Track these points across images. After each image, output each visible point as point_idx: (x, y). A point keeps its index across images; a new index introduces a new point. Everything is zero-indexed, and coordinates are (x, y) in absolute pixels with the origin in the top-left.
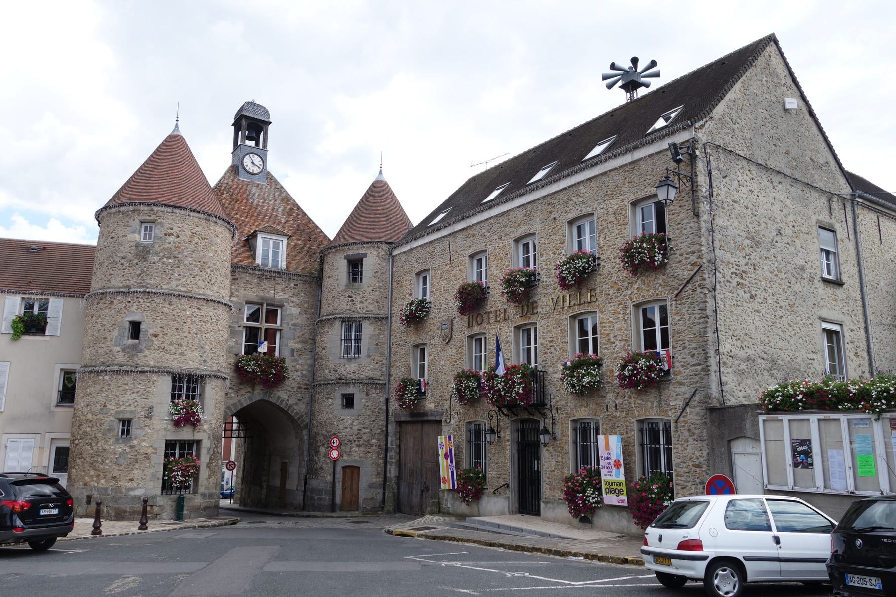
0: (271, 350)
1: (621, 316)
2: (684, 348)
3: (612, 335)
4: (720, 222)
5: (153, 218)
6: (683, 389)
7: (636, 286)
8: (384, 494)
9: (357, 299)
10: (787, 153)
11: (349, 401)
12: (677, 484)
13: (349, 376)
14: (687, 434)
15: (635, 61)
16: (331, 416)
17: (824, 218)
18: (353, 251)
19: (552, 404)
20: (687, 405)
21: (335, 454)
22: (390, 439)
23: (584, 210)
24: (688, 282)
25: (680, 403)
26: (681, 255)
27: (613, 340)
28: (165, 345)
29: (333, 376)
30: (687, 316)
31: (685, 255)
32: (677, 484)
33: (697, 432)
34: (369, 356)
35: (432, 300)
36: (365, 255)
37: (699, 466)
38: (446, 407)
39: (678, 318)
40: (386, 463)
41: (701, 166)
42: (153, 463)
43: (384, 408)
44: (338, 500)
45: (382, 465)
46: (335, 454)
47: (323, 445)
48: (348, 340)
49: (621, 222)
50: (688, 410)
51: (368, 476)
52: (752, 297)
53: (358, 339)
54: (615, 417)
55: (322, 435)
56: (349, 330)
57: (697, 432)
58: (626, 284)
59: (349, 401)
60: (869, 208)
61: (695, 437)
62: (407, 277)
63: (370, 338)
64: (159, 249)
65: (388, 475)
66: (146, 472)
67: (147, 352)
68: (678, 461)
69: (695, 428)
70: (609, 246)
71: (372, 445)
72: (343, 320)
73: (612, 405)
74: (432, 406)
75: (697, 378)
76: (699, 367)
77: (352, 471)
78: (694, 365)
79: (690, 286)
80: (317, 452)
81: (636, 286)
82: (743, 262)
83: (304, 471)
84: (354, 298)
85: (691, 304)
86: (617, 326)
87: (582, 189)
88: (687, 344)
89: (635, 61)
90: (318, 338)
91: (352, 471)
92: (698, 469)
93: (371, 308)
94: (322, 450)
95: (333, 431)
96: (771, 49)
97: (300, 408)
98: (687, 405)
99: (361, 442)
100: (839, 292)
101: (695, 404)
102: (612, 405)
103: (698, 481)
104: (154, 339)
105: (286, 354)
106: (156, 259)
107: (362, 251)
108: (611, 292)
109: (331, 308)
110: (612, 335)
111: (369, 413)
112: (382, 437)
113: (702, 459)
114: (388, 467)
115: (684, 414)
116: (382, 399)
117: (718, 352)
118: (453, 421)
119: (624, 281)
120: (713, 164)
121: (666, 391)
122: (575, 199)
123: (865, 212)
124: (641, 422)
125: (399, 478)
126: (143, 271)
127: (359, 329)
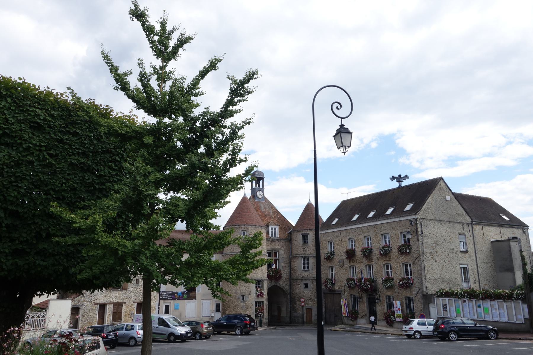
0: (276, 266)
4: (425, 241)
6: (416, 289)
9: (307, 249)
10: (447, 214)
11: (306, 286)
17: (461, 231)
21: (303, 304)
25: (416, 293)
36: (309, 234)
38: (343, 289)
41: (419, 226)
44: (305, 320)
46: (303, 304)
48: (304, 264)
52: (436, 261)
53: (308, 264)
56: (304, 260)
59: (306, 286)
60: (478, 224)
62: (325, 242)
72: (302, 257)
74: (337, 288)
77: (309, 310)
80: (295, 303)
82: (433, 251)
83: (289, 309)
90: (292, 263)
91: (309, 310)
93: (312, 253)
94: (298, 303)
96: (441, 182)
97: (287, 287)
100: (467, 255)
105: (281, 268)
107: (308, 232)
117: (425, 279)
120: (423, 224)
123: (477, 226)
124: (405, 297)
125: (325, 312)
127: (308, 260)
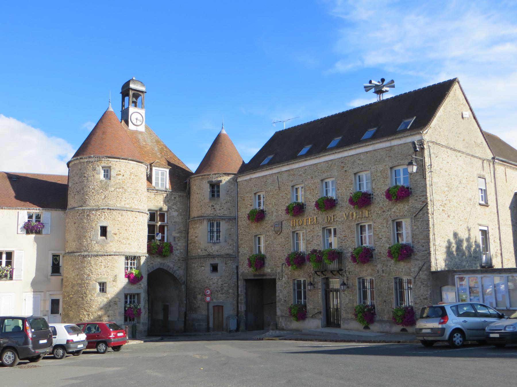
0: (163, 237)
4: (434, 180)
6: (419, 262)
7: (393, 210)
9: (217, 207)
10: (464, 140)
11: (215, 268)
13: (214, 254)
14: (420, 284)
16: (204, 277)
20: (420, 270)
21: (208, 299)
22: (240, 289)
24: (421, 210)
25: (417, 269)
26: (417, 197)
27: (380, 237)
28: (121, 239)
30: (420, 227)
34: (226, 241)
37: (426, 299)
38: (279, 270)
40: (238, 303)
41: (426, 152)
43: (236, 271)
44: (211, 325)
45: (236, 304)
46: (208, 299)
47: (199, 294)
48: (212, 232)
50: (421, 272)
51: (229, 311)
52: (448, 216)
53: (218, 231)
54: (383, 276)
56: (212, 225)
57: (425, 283)
59: (215, 268)
60: (501, 165)
62: (249, 195)
65: (240, 309)
70: (378, 189)
71: (230, 293)
72: (209, 220)
74: (269, 270)
75: (425, 257)
77: (219, 308)
79: (421, 212)
80: (195, 298)
82: (445, 199)
83: (183, 309)
85: (422, 221)
86: (383, 230)
90: (191, 231)
91: (219, 308)
93: (226, 213)
94: (199, 297)
95: (206, 286)
96: (456, 86)
97: (180, 273)
98: (420, 270)
99: (224, 291)
100: (487, 209)
102: (380, 270)
104: (115, 236)
105: (171, 240)
106: (113, 189)
107: (219, 179)
108: (379, 212)
109: (200, 213)
111: (227, 274)
112: (235, 288)
113: (427, 296)
114: (239, 305)
116: (234, 267)
117: (434, 245)
118: (284, 279)
120: (432, 151)
122: (358, 162)
123: (499, 166)
124: (396, 278)
125: (246, 311)
127: (218, 225)
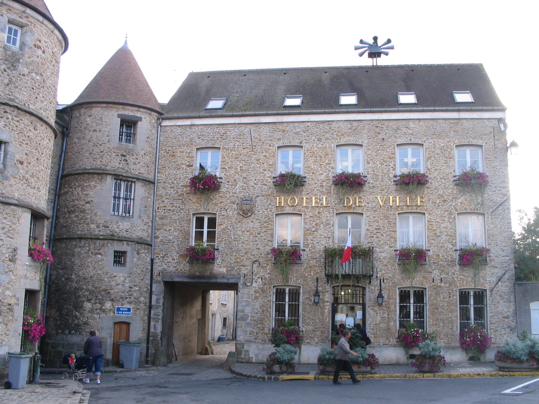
1: (446, 219)
2: (497, 245)
3: (438, 231)
5: (24, 21)
6: (496, 270)
7: (460, 201)
8: (148, 348)
11: (119, 258)
12: (491, 329)
13: (121, 234)
14: (499, 298)
15: (375, 39)
16: (100, 272)
18: (129, 112)
19: (378, 275)
20: (499, 280)
22: (154, 298)
23: (413, 140)
24: (500, 205)
25: (494, 279)
26: (496, 187)
27: (438, 234)
28: (27, 176)
29: (103, 232)
30: (499, 226)
31: (498, 188)
32: (491, 329)
33: (505, 297)
34: (140, 217)
35: (222, 175)
36: (140, 119)
37: (507, 317)
39: (492, 226)
40: (149, 318)
42: (15, 315)
43: (150, 268)
45: (147, 321)
47: (89, 300)
49: (447, 156)
50: (500, 283)
51: (137, 333)
54: (440, 287)
55: (88, 290)
57: (505, 297)
58: (451, 198)
59: (119, 258)
61: (505, 300)
63: (141, 200)
64: (29, 60)
65: (152, 330)
66: (9, 327)
67: (12, 181)
68: (492, 315)
69: (505, 295)
70: (437, 170)
71: (140, 302)
73: (437, 278)
74: (224, 270)
75: (506, 264)
76: (507, 258)
78: (503, 256)
79: (501, 208)
81: (460, 201)
84: (127, 158)
85: (502, 219)
86: (442, 225)
87: (411, 124)
88: (499, 243)
89: (375, 39)
92: (506, 320)
93: (142, 171)
95: (103, 287)
98: (499, 280)
99: (132, 299)
101: (505, 280)
102: (437, 278)
103: (506, 326)
104: (20, 166)
106: (26, 71)
107: (138, 115)
108: (438, 201)
109: (99, 163)
110: (438, 231)
111: (139, 271)
112: (147, 295)
113: (509, 314)
114: (152, 323)
115: (497, 286)
116: (149, 260)
118: (254, 284)
119: (449, 196)
121: (484, 271)
122: (404, 130)
126: (10, 81)
127: (128, 189)
